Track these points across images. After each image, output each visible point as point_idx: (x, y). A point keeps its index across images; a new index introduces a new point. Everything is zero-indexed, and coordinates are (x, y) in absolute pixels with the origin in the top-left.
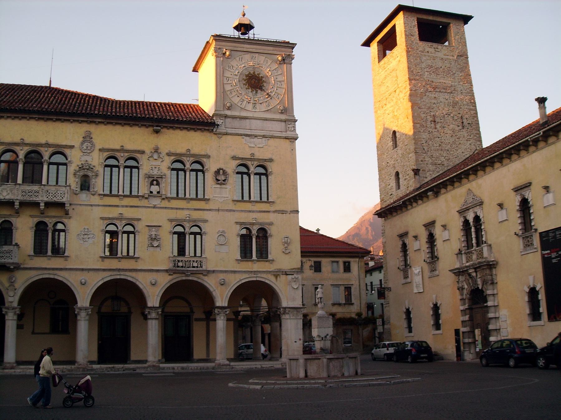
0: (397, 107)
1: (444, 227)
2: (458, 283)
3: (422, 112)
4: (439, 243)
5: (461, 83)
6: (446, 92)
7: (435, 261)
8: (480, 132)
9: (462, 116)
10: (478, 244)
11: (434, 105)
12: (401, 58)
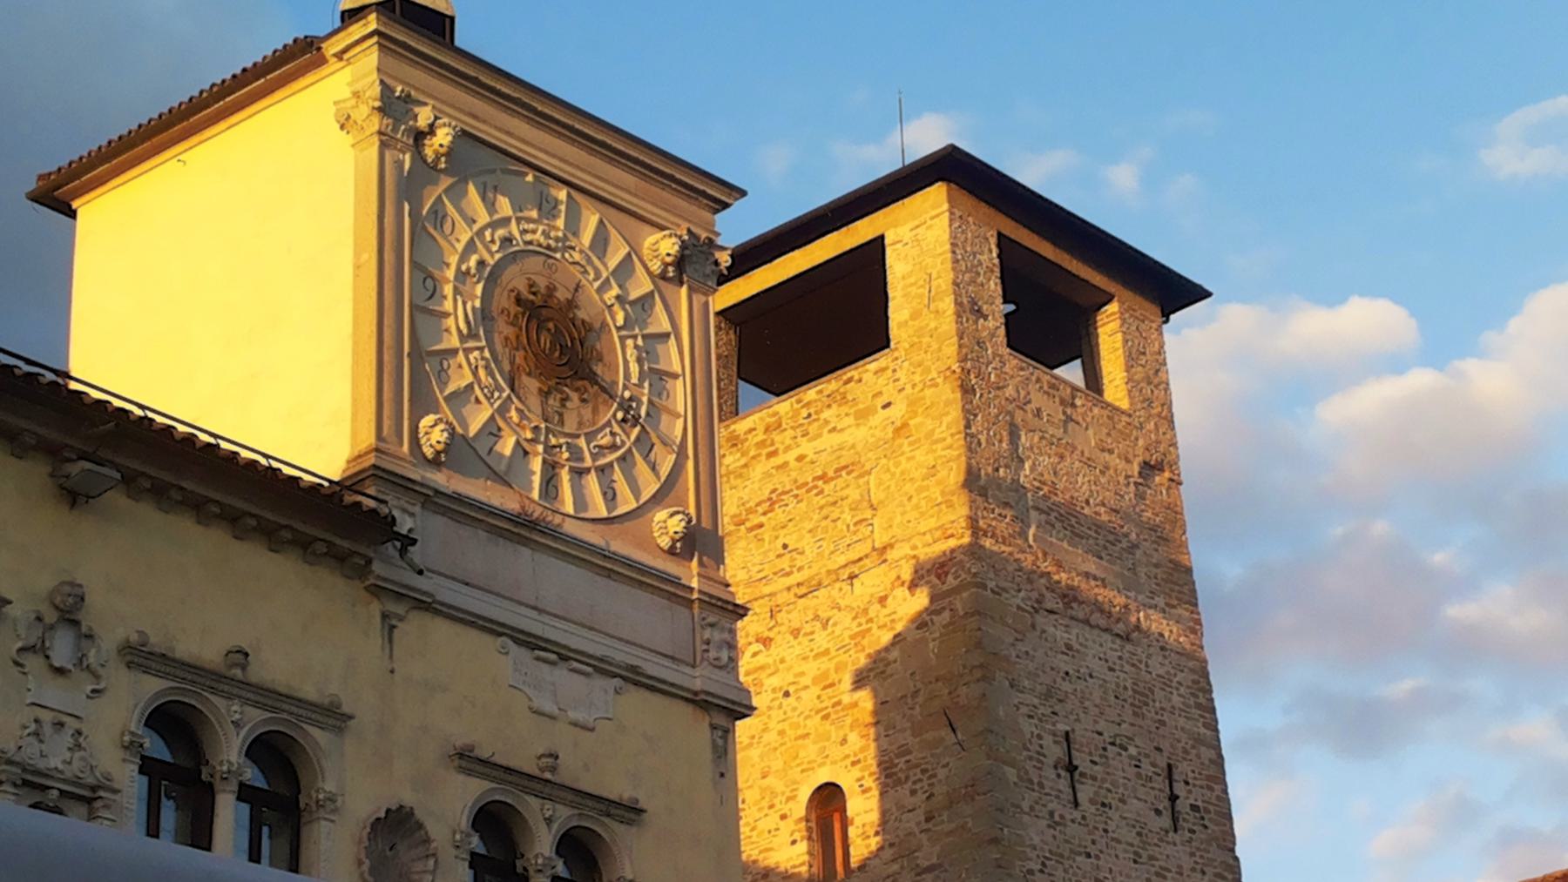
3: (1024, 710)
6: (1106, 630)
8: (1237, 859)
9: (1170, 767)
11: (1066, 686)
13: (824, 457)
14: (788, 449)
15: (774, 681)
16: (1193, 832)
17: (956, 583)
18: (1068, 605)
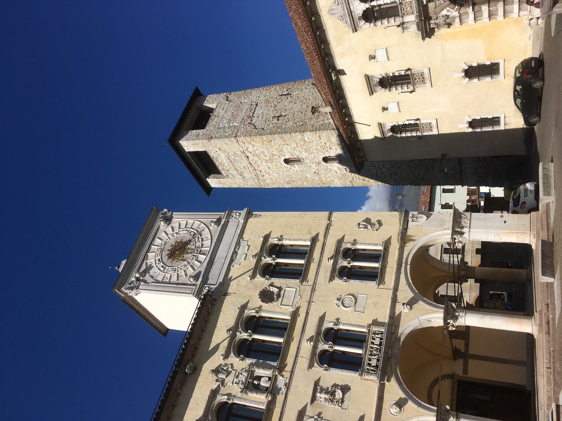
0: (262, 155)
3: (268, 127)
5: (250, 97)
6: (255, 109)
7: (412, 74)
13: (227, 162)
14: (227, 167)
15: (267, 170)
16: (291, 91)
17: (245, 140)
18: (250, 117)
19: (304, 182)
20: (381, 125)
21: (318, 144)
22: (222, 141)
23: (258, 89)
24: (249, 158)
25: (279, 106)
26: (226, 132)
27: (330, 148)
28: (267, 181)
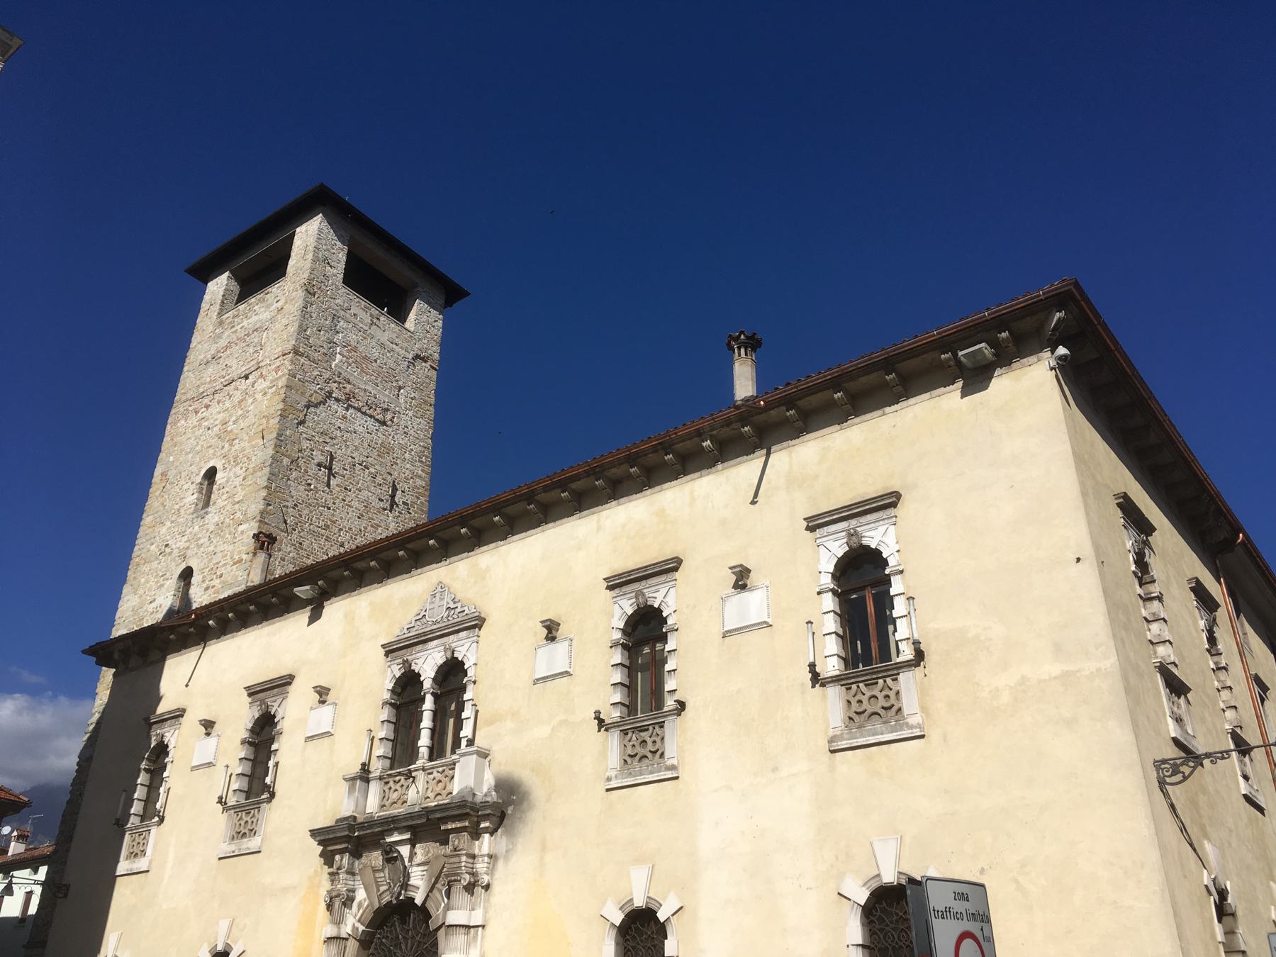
0: (240, 412)
1: (322, 693)
2: (332, 881)
3: (304, 435)
4: (287, 750)
5: (411, 413)
6: (371, 416)
7: (259, 803)
10: (436, 751)
11: (339, 434)
12: (286, 303)
14: (239, 324)
15: (206, 424)
16: (401, 513)
18: (348, 399)
19: (156, 515)
20: (178, 714)
21: (226, 556)
22: (295, 316)
23: (430, 437)
24: (243, 381)
25: (362, 476)
26: (320, 331)
27: (207, 589)
28: (183, 422)
